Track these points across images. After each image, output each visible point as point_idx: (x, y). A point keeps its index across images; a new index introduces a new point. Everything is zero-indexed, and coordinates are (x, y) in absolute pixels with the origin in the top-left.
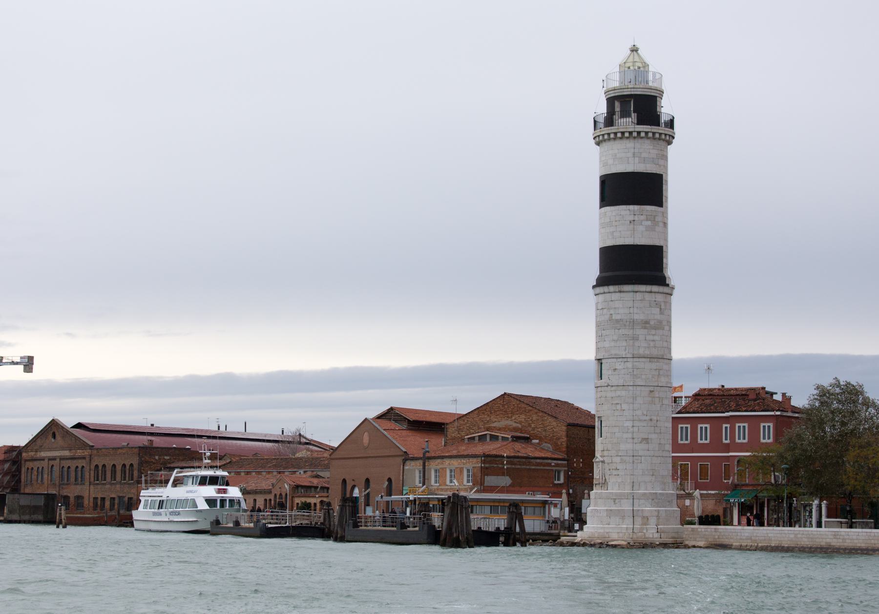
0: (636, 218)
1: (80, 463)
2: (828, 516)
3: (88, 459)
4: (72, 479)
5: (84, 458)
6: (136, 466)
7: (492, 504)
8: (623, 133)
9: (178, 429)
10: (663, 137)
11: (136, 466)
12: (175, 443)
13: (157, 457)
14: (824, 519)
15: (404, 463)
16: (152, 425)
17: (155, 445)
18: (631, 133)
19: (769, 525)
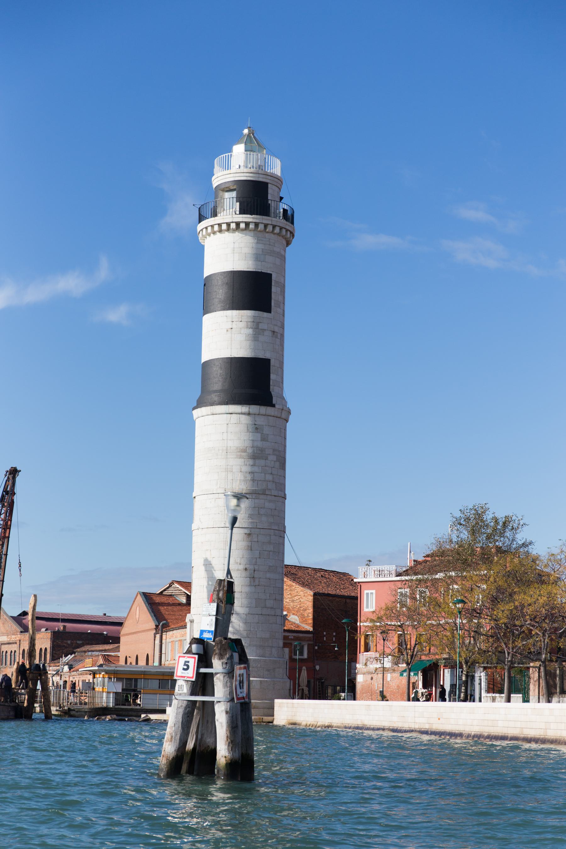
0: (234, 326)
1: (14, 647)
2: (488, 691)
3: (18, 643)
4: (8, 663)
5: (16, 643)
6: (48, 650)
7: (161, 677)
8: (220, 225)
9: (88, 616)
10: (270, 228)
11: (48, 650)
12: (90, 628)
13: (69, 642)
14: (484, 694)
15: (155, 637)
16: (105, 614)
17: (67, 630)
18: (228, 225)
19: (450, 701)
